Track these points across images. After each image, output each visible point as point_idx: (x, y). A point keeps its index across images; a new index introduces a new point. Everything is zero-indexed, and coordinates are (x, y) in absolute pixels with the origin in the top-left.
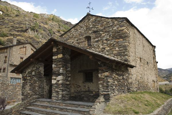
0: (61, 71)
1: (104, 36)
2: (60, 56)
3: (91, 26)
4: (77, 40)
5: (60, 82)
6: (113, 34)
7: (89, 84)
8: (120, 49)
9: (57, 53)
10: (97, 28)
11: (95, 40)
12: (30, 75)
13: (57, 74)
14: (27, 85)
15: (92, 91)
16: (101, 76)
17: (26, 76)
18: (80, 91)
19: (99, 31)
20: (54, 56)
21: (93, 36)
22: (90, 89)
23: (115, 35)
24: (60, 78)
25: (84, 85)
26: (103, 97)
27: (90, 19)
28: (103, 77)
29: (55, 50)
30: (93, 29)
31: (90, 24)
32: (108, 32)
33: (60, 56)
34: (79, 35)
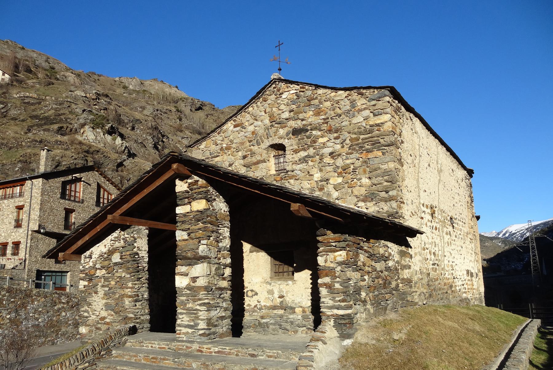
1: (324, 144)
2: (200, 205)
3: (286, 115)
5: (201, 282)
6: (354, 136)
7: (281, 287)
8: (375, 181)
9: (190, 197)
10: (302, 120)
11: (299, 154)
12: (106, 263)
13: (189, 259)
14: (96, 293)
15: (293, 305)
16: (326, 261)
17: (94, 268)
18: (256, 306)
19: (309, 128)
20: (178, 205)
21: (290, 143)
22: (287, 299)
23: (358, 139)
24: (199, 269)
25: (269, 287)
26: (332, 323)
27: (282, 94)
28: (332, 265)
29: (181, 186)
31: (282, 107)
33: (200, 205)
34: (250, 141)
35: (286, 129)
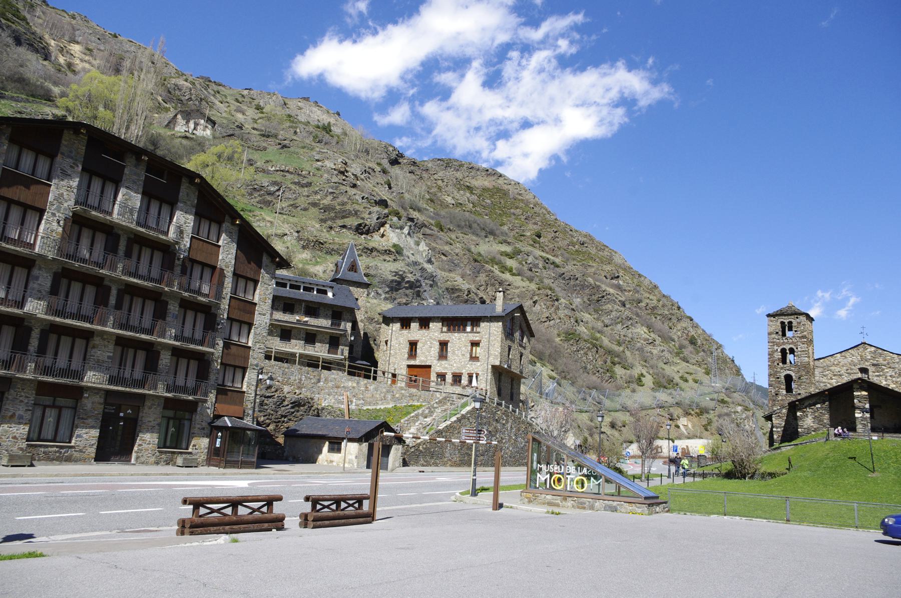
0: (867, 406)
1: (887, 372)
3: (869, 357)
4: (847, 370)
30: (871, 361)
32: (893, 368)
35: (869, 363)
